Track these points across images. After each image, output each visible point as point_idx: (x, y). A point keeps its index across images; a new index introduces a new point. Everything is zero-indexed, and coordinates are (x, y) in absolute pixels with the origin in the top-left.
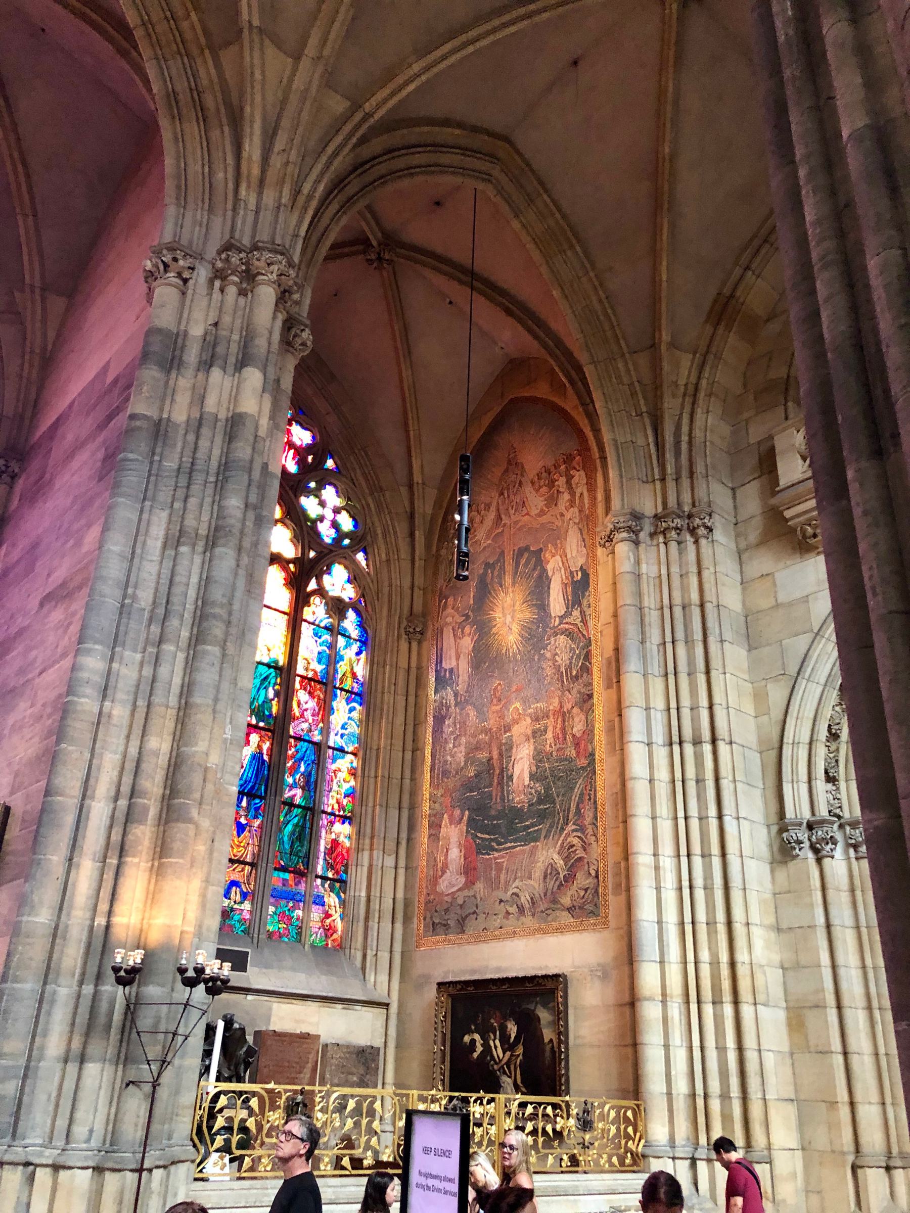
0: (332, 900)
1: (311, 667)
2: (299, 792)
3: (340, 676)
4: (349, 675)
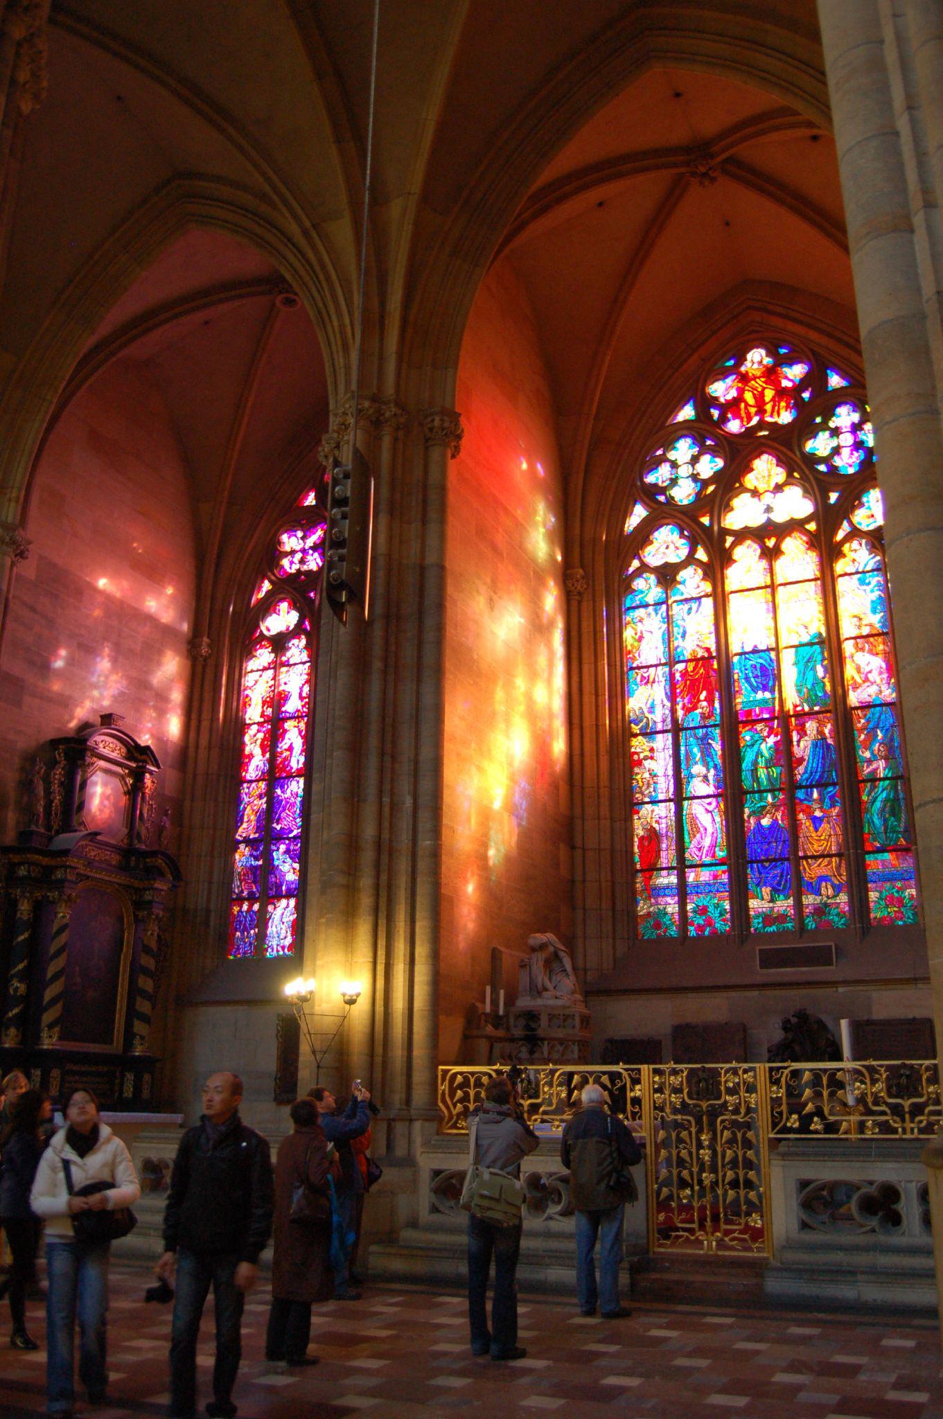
2: (882, 763)
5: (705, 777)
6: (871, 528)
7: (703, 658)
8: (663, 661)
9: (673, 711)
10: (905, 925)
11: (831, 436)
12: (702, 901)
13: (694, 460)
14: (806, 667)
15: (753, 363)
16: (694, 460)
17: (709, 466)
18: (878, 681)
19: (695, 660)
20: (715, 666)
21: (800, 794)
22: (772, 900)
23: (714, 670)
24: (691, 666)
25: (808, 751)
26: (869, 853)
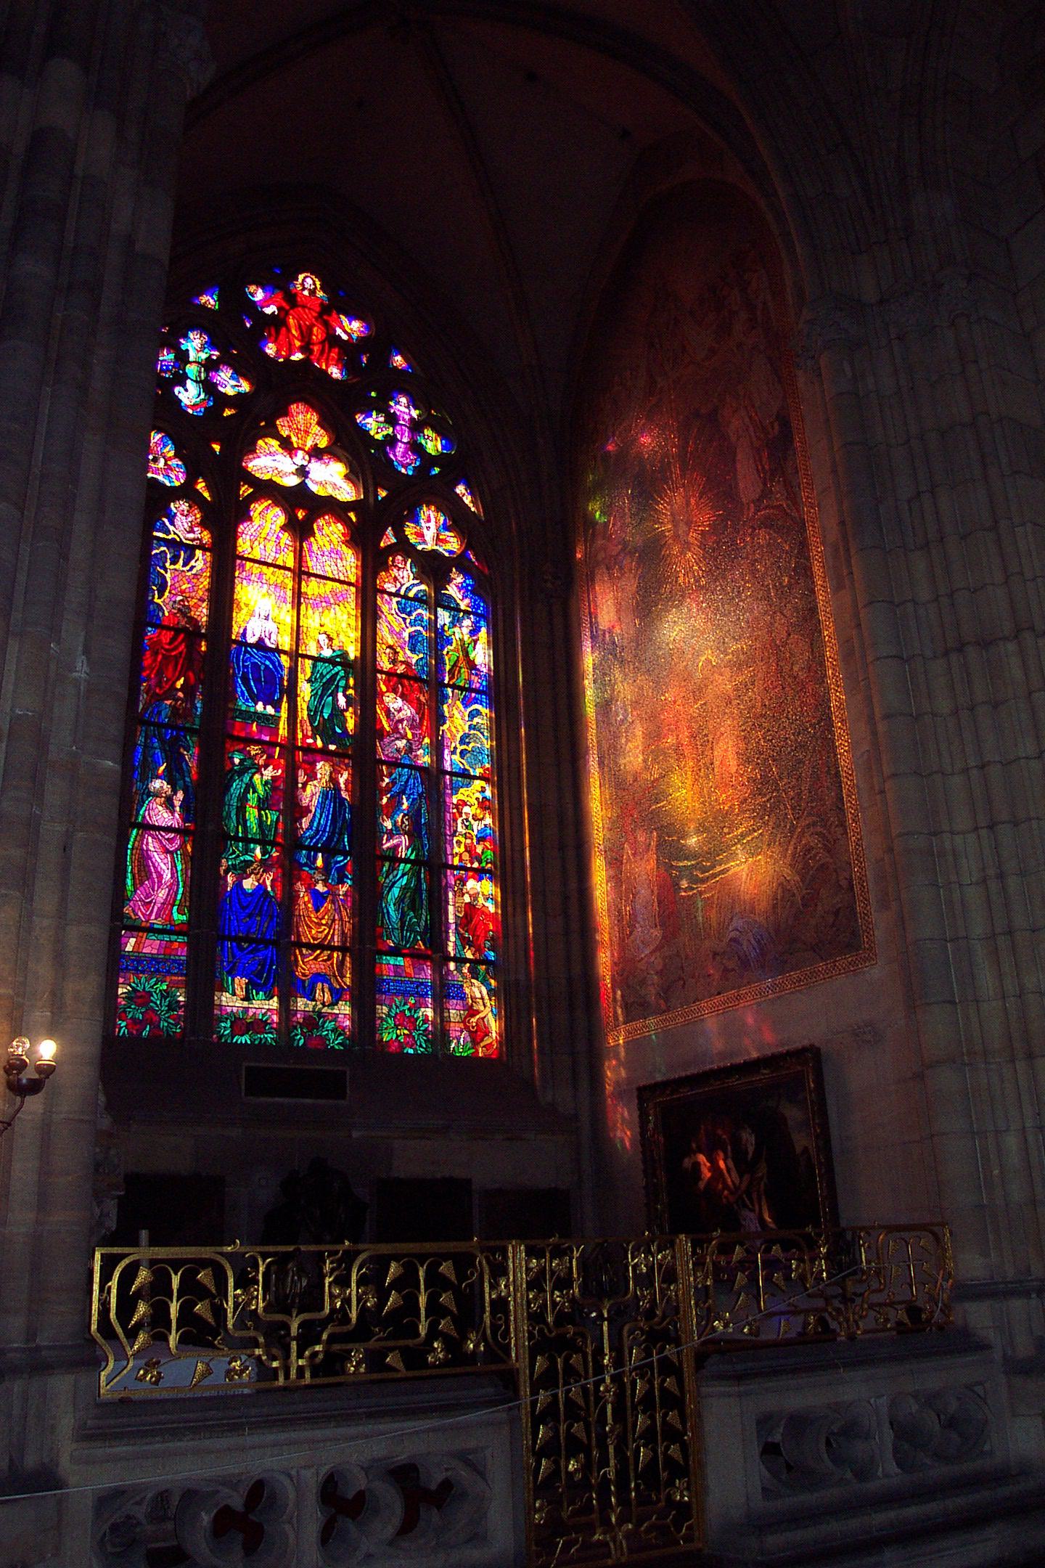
0: (477, 990)
2: (404, 840)
4: (462, 664)
7: (185, 629)
10: (416, 1054)
12: (145, 983)
14: (326, 686)
15: (304, 289)
16: (210, 366)
18: (410, 736)
19: (177, 631)
22: (247, 998)
24: (166, 637)
25: (315, 802)
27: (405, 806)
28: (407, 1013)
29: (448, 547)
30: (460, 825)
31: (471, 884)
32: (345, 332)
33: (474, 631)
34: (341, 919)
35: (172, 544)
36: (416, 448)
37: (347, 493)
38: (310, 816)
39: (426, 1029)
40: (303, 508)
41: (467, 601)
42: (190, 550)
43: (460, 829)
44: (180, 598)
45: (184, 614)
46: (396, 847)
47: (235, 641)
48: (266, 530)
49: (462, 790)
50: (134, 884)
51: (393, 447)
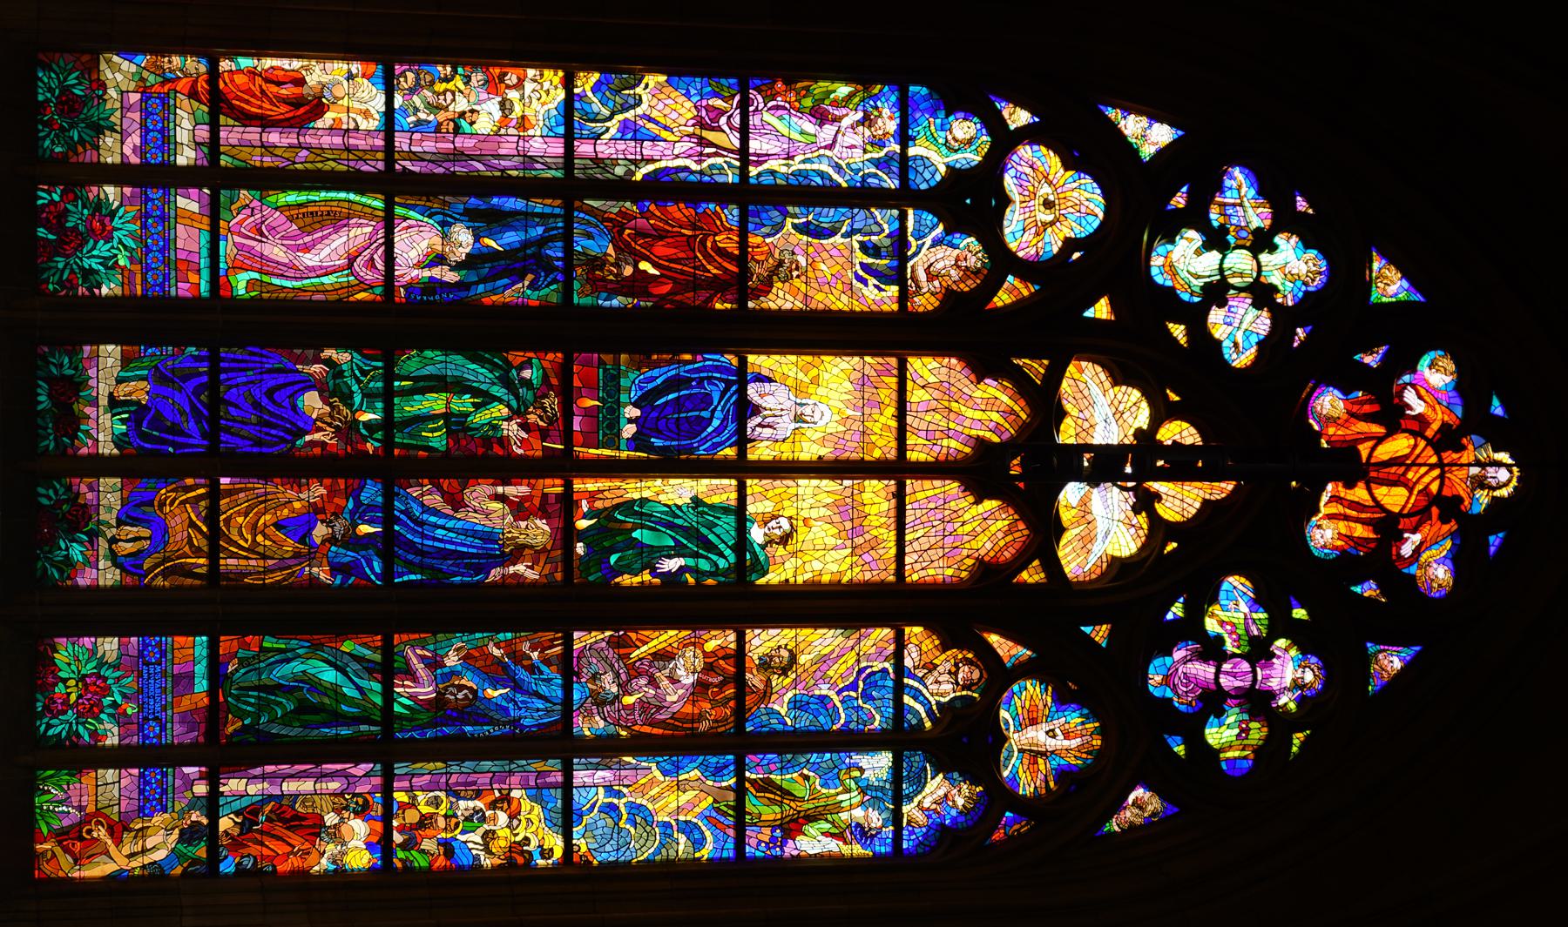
1: (775, 680)
2: (426, 691)
3: (775, 777)
4: (789, 807)
5: (439, 260)
6: (1003, 714)
7: (745, 273)
8: (753, 171)
9: (622, 188)
11: (1253, 640)
12: (125, 227)
13: (1261, 294)
14: (687, 531)
16: (1261, 294)
17: (1239, 331)
19: (743, 258)
20: (718, 306)
21: (371, 493)
22: (114, 403)
23: (710, 300)
25: (476, 519)
26: (213, 647)
27: (492, 693)
28: (107, 701)
29: (1024, 778)
30: (471, 804)
31: (359, 829)
32: (1417, 552)
33: (862, 833)
34: (268, 571)
35: (900, 242)
36: (1213, 701)
37: (1076, 561)
38: (448, 510)
39: (79, 736)
40: (1025, 469)
41: (920, 817)
42: (898, 276)
43: (462, 804)
44: (802, 261)
45: (774, 271)
46: (411, 674)
47: (743, 362)
48: (970, 413)
49: (537, 809)
50: (289, 206)
51: (1203, 657)
